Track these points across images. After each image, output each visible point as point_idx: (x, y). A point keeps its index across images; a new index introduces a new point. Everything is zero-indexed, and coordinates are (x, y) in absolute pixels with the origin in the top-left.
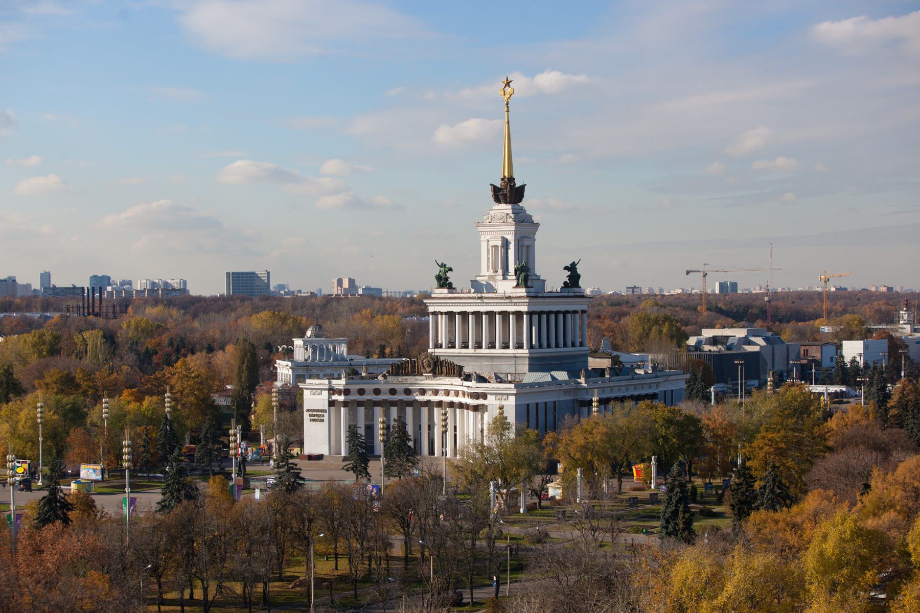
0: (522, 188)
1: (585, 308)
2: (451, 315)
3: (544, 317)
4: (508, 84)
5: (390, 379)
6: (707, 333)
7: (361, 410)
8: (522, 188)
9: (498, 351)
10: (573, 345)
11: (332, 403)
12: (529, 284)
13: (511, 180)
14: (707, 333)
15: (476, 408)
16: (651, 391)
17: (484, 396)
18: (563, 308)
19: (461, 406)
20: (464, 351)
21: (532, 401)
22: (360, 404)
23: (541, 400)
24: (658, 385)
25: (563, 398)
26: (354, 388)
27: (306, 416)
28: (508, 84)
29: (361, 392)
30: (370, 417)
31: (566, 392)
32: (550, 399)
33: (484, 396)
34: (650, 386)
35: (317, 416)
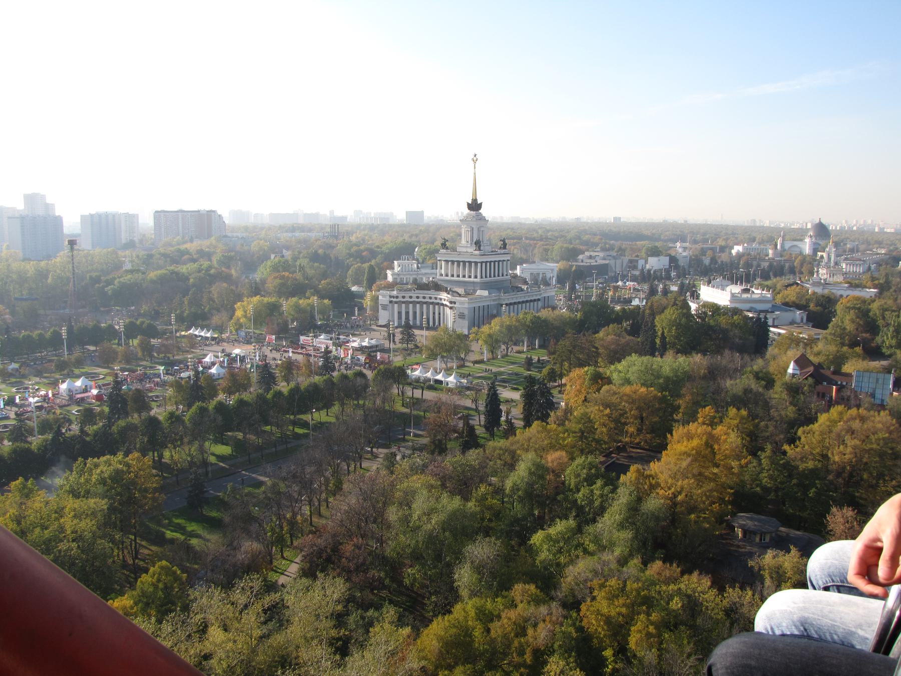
0: (481, 204)
1: (509, 258)
2: (447, 261)
3: (488, 264)
4: (475, 155)
5: (416, 291)
6: (587, 254)
7: (403, 305)
8: (481, 204)
9: (467, 279)
10: (503, 275)
11: (391, 302)
12: (482, 248)
13: (475, 200)
14: (587, 254)
15: (451, 308)
16: (536, 298)
17: (455, 303)
18: (498, 259)
19: (446, 306)
20: (452, 278)
21: (477, 305)
22: (403, 302)
23: (481, 305)
24: (541, 294)
25: (492, 303)
26: (400, 295)
27: (380, 307)
28: (475, 155)
29: (404, 297)
30: (407, 308)
31: (494, 300)
32: (486, 304)
33: (455, 303)
34: (536, 295)
35: (385, 307)
